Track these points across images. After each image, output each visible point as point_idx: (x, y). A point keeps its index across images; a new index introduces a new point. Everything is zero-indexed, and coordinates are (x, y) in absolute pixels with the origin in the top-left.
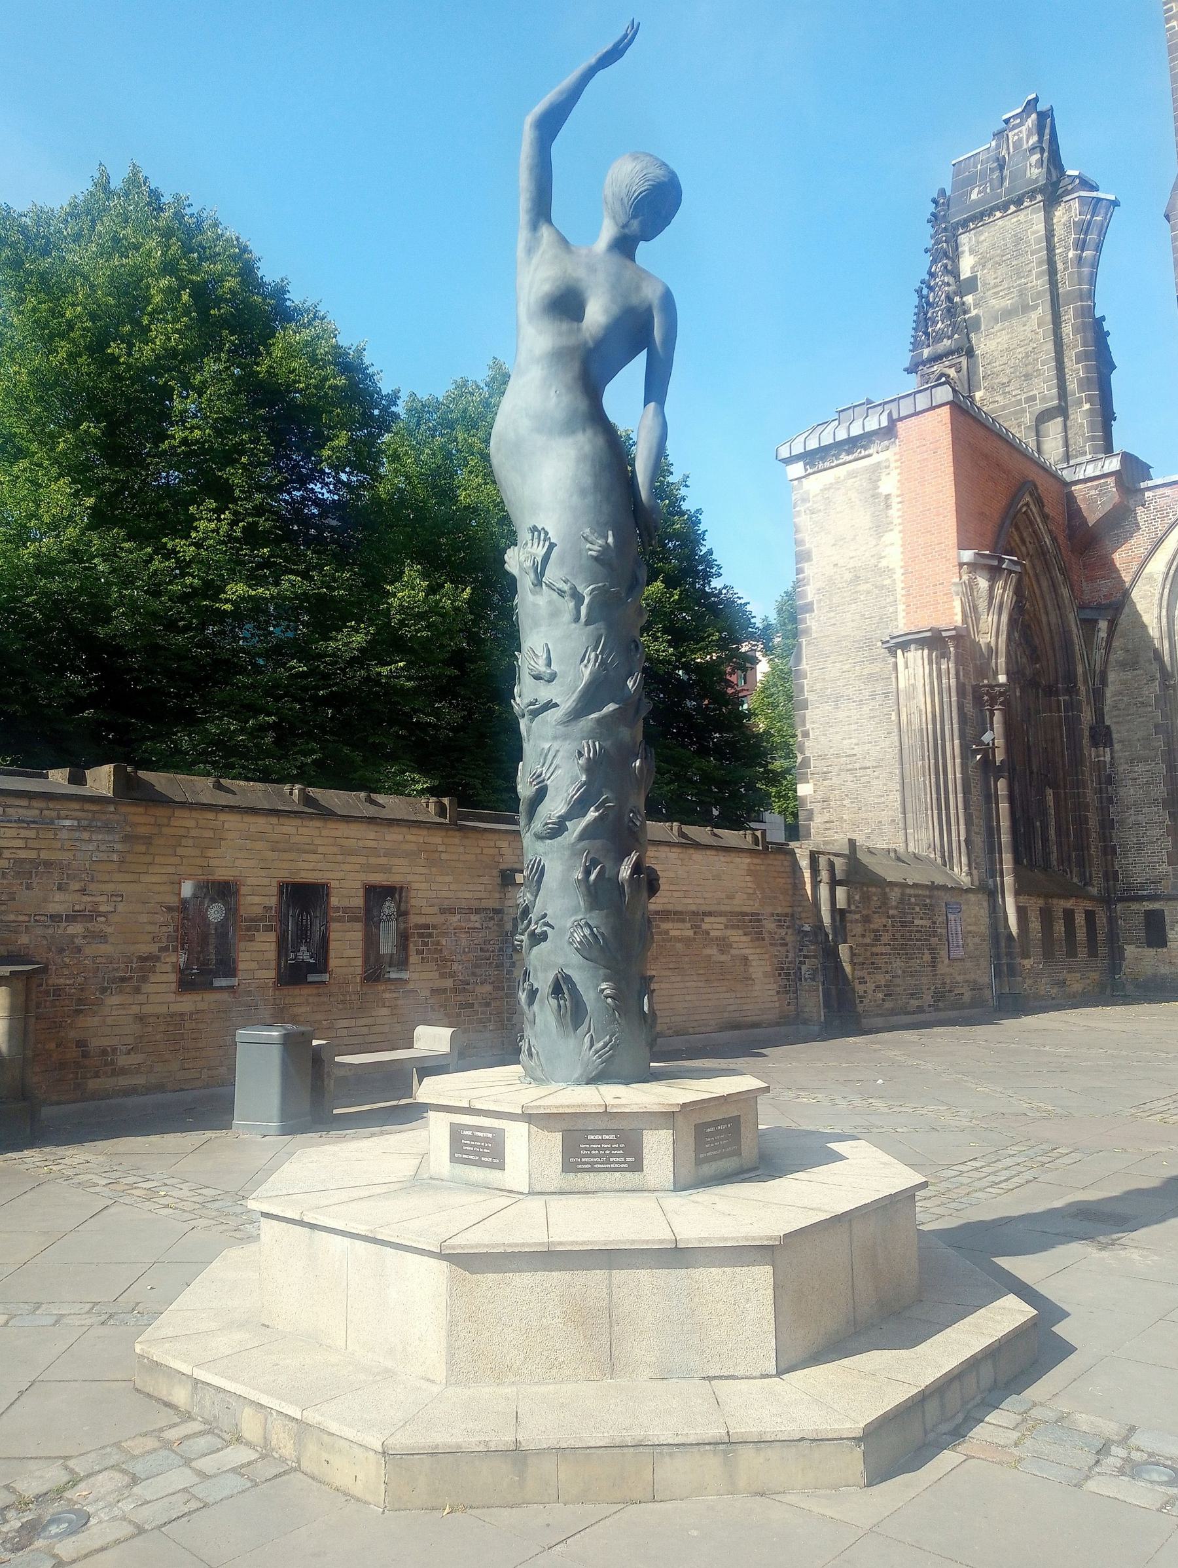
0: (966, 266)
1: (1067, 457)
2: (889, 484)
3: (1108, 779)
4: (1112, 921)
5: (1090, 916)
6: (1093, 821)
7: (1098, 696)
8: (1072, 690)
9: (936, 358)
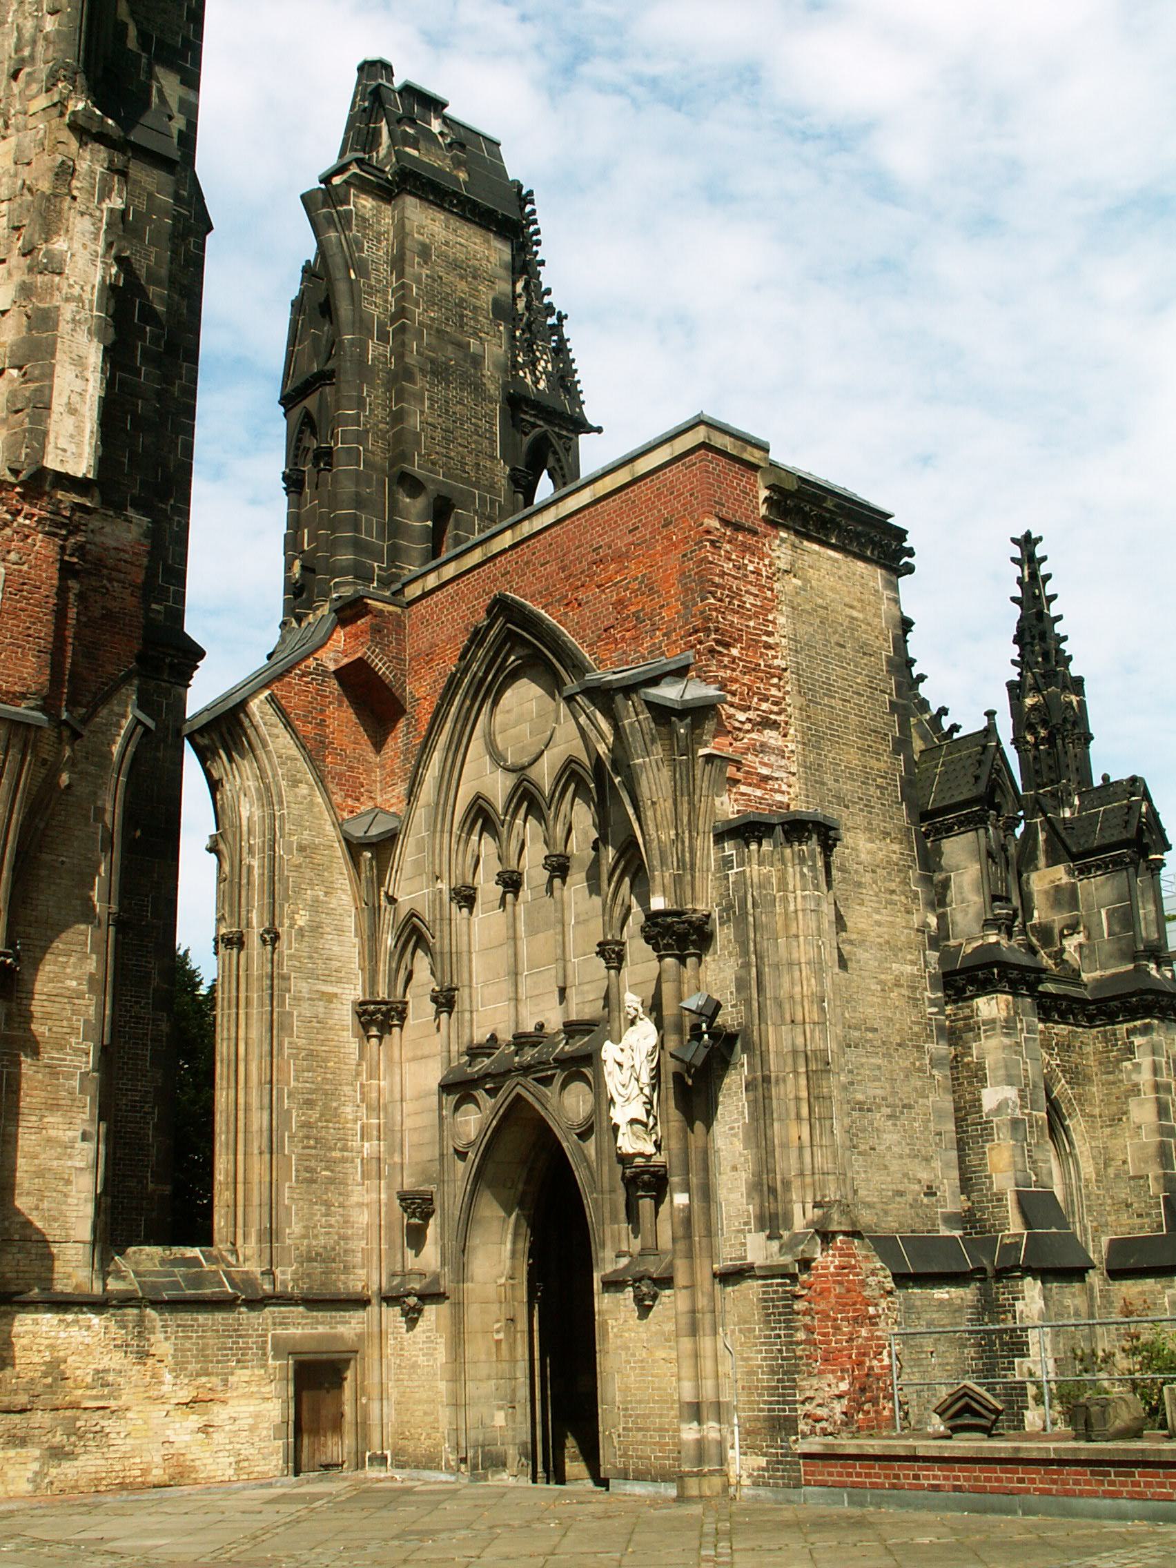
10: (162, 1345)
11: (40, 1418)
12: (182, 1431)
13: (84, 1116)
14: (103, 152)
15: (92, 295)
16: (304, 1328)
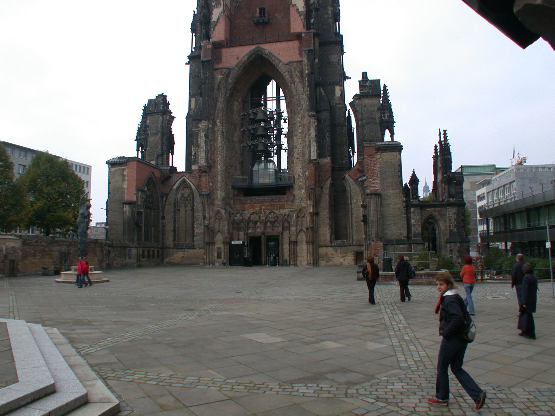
0: (148, 121)
1: (162, 164)
2: (125, 173)
3: (164, 226)
4: (163, 252)
5: (158, 251)
6: (161, 234)
7: (163, 210)
8: (158, 209)
9: (140, 139)
10: (339, 251)
11: (325, 258)
12: (342, 260)
13: (328, 227)
14: (313, 118)
15: (314, 137)
16: (356, 249)
